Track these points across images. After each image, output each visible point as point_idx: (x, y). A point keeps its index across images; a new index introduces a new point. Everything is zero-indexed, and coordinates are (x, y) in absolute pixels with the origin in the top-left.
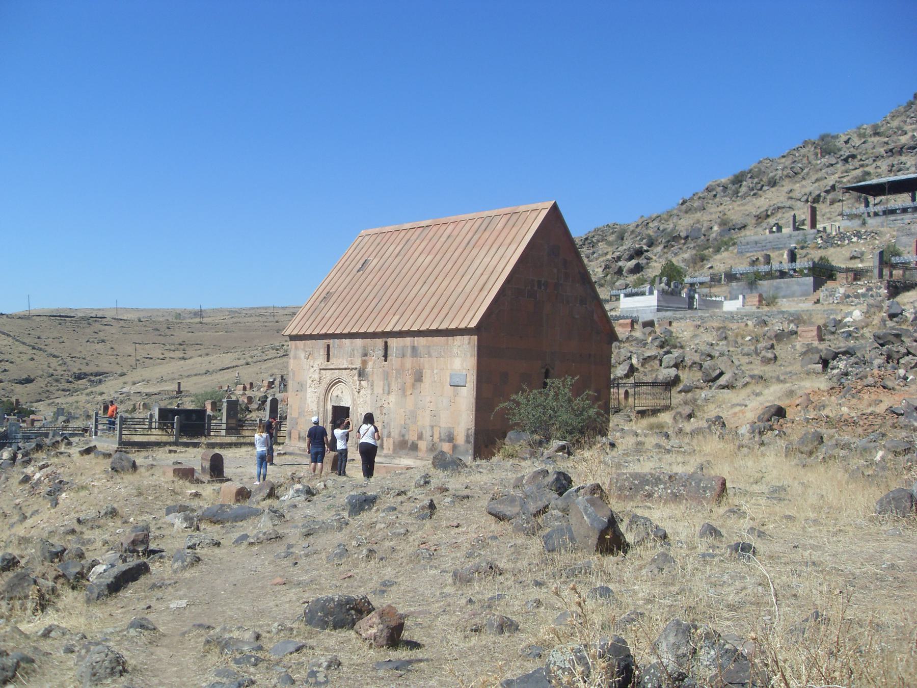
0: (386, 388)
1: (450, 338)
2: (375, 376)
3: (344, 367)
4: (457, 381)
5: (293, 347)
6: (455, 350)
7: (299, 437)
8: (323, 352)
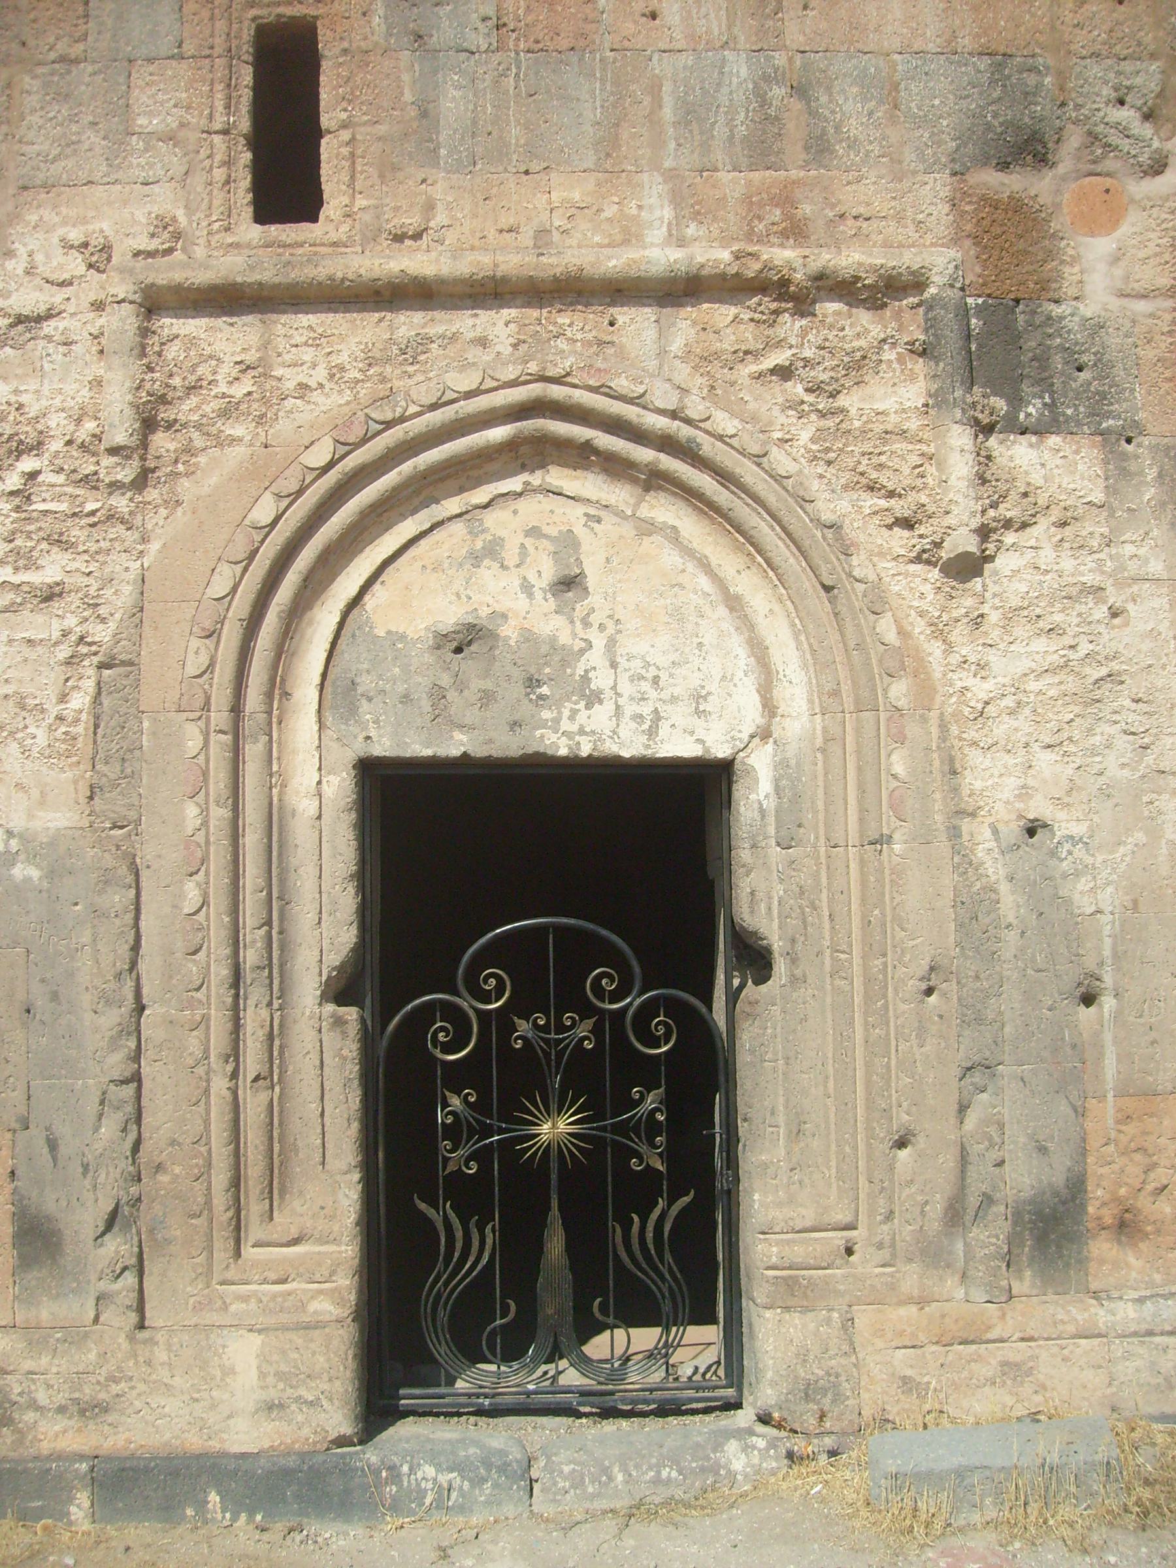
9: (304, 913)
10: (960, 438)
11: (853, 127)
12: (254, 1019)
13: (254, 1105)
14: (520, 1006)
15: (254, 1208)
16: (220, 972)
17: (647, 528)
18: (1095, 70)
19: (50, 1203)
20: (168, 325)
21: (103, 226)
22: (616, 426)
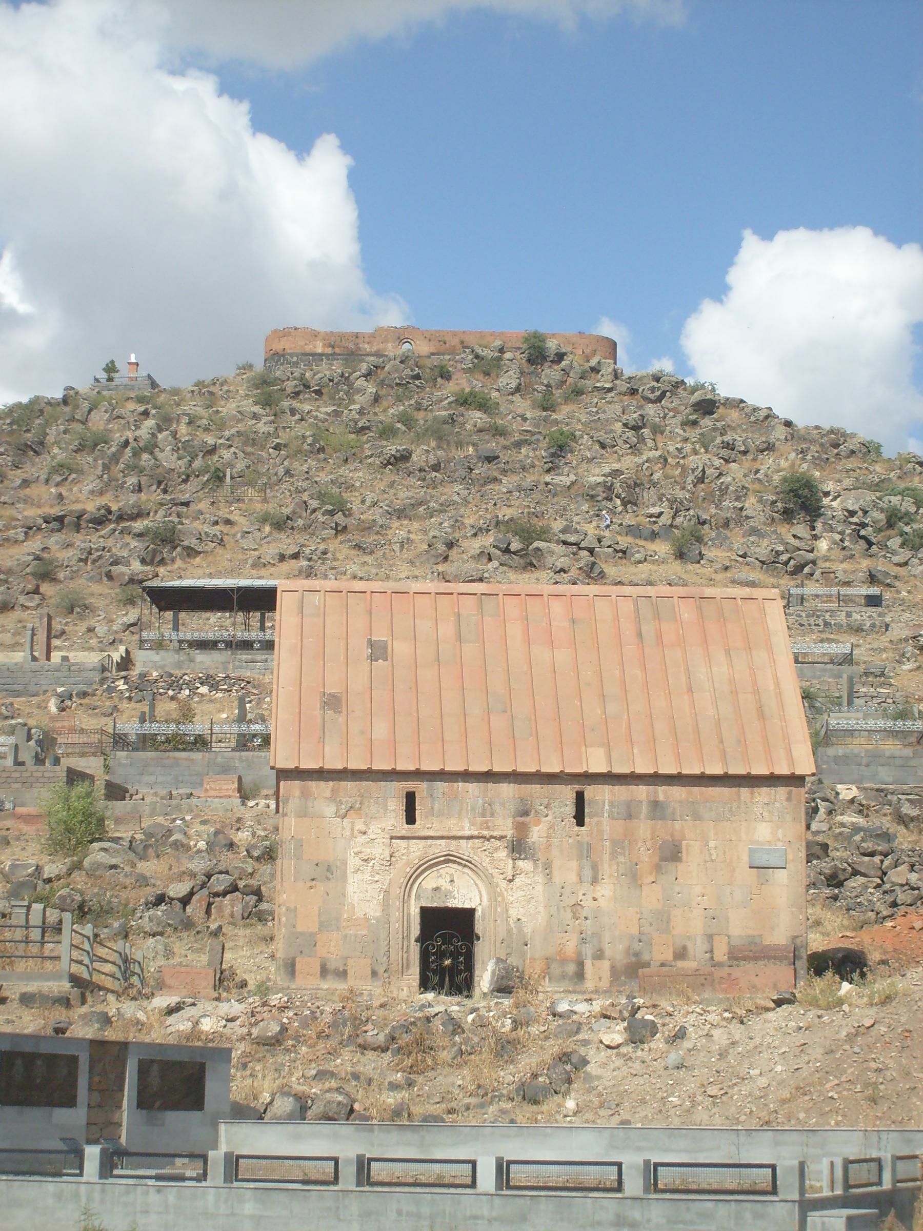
0: (588, 873)
1: (745, 792)
2: (555, 852)
3: (467, 833)
4: (762, 860)
5: (297, 793)
6: (758, 810)
7: (324, 971)
8: (397, 806)
9: (412, 929)
10: (511, 861)
11: (498, 811)
12: (405, 943)
13: (405, 956)
14: (443, 944)
15: (405, 970)
16: (401, 937)
17: (464, 873)
18: (537, 800)
19: (376, 969)
20: (394, 841)
21: (384, 825)
22: (459, 858)
